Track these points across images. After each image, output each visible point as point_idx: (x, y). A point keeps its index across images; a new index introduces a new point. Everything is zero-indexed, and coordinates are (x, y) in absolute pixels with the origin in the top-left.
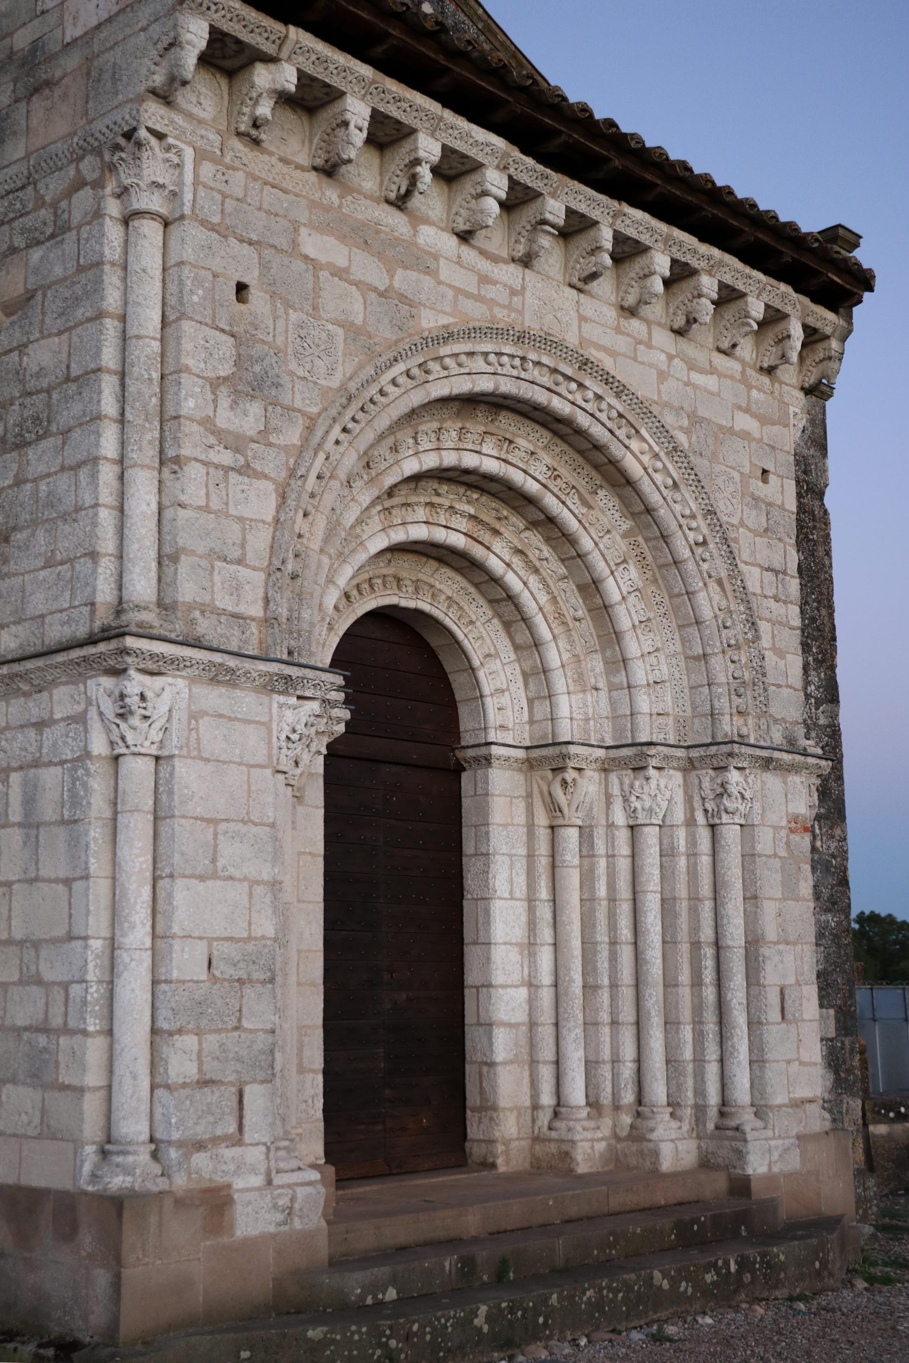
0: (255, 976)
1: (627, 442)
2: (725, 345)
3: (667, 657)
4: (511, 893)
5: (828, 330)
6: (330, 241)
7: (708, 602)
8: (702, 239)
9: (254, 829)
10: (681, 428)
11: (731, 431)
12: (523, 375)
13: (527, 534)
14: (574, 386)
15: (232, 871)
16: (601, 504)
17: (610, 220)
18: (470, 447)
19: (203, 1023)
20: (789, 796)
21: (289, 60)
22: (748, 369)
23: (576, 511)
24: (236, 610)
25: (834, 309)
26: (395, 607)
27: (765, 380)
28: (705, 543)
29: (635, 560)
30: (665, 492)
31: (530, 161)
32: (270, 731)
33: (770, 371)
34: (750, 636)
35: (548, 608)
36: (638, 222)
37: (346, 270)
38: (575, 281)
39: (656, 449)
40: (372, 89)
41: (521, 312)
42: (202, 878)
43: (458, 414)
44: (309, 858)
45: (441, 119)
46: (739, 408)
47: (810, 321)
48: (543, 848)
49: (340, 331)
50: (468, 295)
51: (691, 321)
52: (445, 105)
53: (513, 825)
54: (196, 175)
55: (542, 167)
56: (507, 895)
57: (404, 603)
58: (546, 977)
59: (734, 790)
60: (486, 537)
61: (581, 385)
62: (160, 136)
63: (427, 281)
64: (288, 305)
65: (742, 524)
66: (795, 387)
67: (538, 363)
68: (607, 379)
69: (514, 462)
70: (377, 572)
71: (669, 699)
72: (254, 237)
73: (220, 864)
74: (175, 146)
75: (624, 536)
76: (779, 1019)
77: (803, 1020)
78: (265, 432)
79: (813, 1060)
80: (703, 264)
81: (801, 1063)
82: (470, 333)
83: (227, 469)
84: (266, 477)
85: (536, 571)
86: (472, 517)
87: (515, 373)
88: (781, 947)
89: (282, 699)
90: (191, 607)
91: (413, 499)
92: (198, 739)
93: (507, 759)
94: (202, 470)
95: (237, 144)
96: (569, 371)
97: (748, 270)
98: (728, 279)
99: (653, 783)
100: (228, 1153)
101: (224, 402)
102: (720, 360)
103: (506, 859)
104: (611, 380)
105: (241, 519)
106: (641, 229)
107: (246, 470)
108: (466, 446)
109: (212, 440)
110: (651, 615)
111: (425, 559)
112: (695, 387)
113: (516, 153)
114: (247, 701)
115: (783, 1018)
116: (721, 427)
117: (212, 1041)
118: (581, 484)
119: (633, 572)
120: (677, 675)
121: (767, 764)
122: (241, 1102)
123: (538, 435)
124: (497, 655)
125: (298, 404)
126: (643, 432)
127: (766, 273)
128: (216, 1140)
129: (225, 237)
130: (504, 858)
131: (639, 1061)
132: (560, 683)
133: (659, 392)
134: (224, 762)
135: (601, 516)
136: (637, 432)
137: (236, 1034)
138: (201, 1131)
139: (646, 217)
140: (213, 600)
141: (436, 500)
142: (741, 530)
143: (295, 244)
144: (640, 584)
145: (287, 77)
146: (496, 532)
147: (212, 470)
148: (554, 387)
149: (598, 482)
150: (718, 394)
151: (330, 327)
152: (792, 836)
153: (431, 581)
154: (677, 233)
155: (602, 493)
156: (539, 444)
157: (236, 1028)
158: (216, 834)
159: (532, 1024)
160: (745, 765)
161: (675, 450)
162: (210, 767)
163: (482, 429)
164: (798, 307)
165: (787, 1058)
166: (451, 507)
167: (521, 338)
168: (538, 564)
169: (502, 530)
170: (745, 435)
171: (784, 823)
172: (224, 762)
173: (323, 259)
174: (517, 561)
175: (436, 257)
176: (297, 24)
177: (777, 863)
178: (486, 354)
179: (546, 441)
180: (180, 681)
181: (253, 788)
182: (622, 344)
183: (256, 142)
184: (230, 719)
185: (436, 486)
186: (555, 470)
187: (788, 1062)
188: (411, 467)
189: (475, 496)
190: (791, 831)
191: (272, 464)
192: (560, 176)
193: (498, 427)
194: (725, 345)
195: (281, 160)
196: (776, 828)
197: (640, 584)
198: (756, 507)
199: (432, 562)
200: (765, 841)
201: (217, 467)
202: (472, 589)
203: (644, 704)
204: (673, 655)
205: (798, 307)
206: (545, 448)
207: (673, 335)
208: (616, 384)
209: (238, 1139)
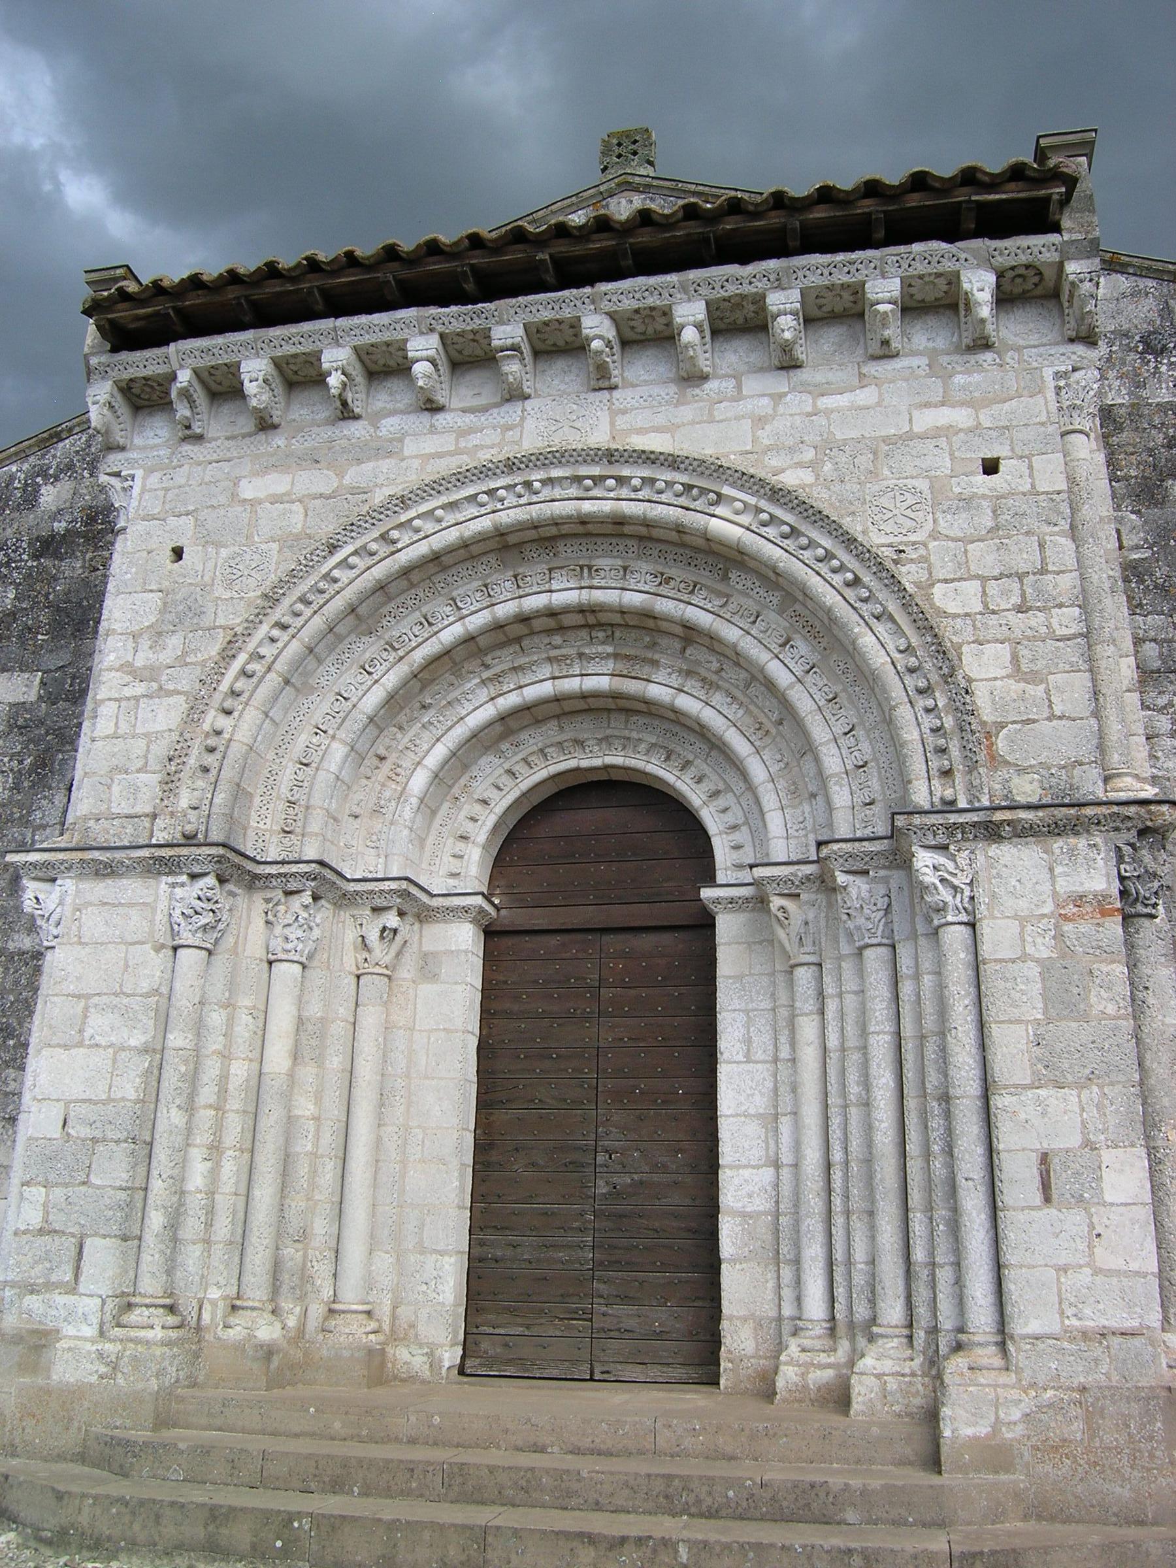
0: (110, 1135)
1: (711, 510)
2: (875, 348)
3: (868, 732)
4: (748, 1055)
5: (1051, 256)
6: (273, 476)
7: (877, 646)
8: (744, 261)
9: (125, 1001)
10: (800, 465)
11: (909, 437)
12: (535, 499)
13: (688, 652)
14: (611, 482)
15: (98, 1039)
16: (739, 587)
17: (592, 307)
18: (535, 589)
19: (52, 1177)
20: (1058, 870)
21: (182, 367)
22: (944, 360)
23: (709, 606)
24: (132, 811)
25: (1056, 228)
26: (577, 769)
27: (989, 356)
28: (856, 582)
29: (804, 632)
30: (786, 543)
31: (454, 309)
32: (154, 910)
33: (983, 344)
34: (946, 670)
35: (748, 720)
36: (631, 292)
37: (288, 494)
38: (593, 383)
39: (752, 500)
40: (260, 345)
41: (518, 443)
42: (66, 1047)
43: (504, 564)
44: (442, 1034)
45: (335, 329)
46: (927, 405)
47: (999, 260)
48: (783, 999)
49: (275, 546)
50: (440, 455)
51: (786, 349)
52: (336, 317)
53: (751, 975)
54: (144, 485)
55: (470, 307)
56: (741, 1057)
57: (585, 764)
58: (786, 1158)
59: (930, 878)
60: (645, 671)
61: (621, 480)
62: (117, 475)
63: (386, 465)
64: (218, 545)
65: (935, 535)
66: (1057, 344)
67: (549, 482)
68: (648, 458)
69: (603, 584)
70: (548, 742)
71: (875, 783)
72: (191, 508)
73: (87, 1035)
74: (129, 475)
75: (781, 613)
76: (1038, 1199)
77: (1104, 1204)
78: (185, 654)
79: (1134, 1266)
80: (760, 285)
81: (1097, 1271)
82: (436, 487)
83: (136, 699)
84: (179, 693)
85: (718, 687)
86: (616, 656)
87: (523, 501)
88: (1042, 1092)
89: (170, 879)
90: (86, 818)
91: (523, 660)
92: (79, 928)
93: (732, 901)
94: (114, 705)
95: (187, 448)
96: (596, 471)
97: (840, 257)
98: (814, 280)
99: (853, 892)
100: (60, 1299)
101: (145, 643)
102: (873, 368)
103: (741, 1018)
104: (652, 456)
105: (146, 735)
106: (637, 296)
107: (163, 692)
108: (528, 590)
109: (128, 678)
110: (838, 688)
111: (605, 715)
112: (828, 412)
113: (433, 311)
114: (131, 888)
115: (1047, 1199)
116: (886, 440)
117: (58, 1193)
118: (704, 577)
119: (802, 647)
120: (883, 749)
121: (991, 832)
122: (80, 1253)
123: (621, 548)
124: (728, 789)
125: (221, 621)
126: (726, 490)
127: (877, 246)
128: (49, 1286)
129: (164, 520)
130: (736, 1014)
131: (872, 1262)
132: (769, 800)
133: (755, 441)
134: (102, 944)
135: (743, 600)
136: (719, 495)
137: (83, 1189)
138: (37, 1274)
139: (641, 280)
140: (109, 808)
141: (554, 653)
142: (932, 545)
143: (234, 495)
144: (815, 658)
145: (184, 377)
146: (655, 663)
147: (124, 704)
148: (585, 495)
149: (720, 566)
150: (879, 404)
151: (264, 546)
152: (1068, 927)
153: (626, 733)
154: (693, 274)
155: (733, 575)
156: (630, 555)
157: (84, 1183)
158: (86, 1008)
159: (777, 1215)
160: (941, 839)
161: (777, 494)
162: (87, 949)
163: (543, 568)
164: (963, 256)
165: (1062, 1262)
166: (581, 655)
167: (510, 466)
168: (714, 678)
169: (656, 657)
170: (947, 431)
171: (1048, 908)
172: (102, 944)
173: (262, 495)
174: (691, 684)
175: (401, 440)
176: (175, 340)
177: (1033, 970)
178: (472, 498)
179: (635, 549)
180: (68, 880)
181: (130, 963)
182: (686, 413)
183: (200, 438)
184: (114, 905)
185: (546, 641)
186: (662, 574)
187: (1063, 1269)
188: (451, 634)
189: (601, 635)
190: (1065, 918)
191: (186, 680)
192: (497, 302)
193: (567, 558)
194: (875, 348)
195: (227, 438)
196: (1022, 921)
197: (815, 658)
198: (967, 509)
199: (613, 716)
200: (998, 937)
201: (128, 699)
202: (677, 729)
203: (841, 796)
204: (874, 728)
205: (963, 256)
206: (639, 557)
207: (783, 373)
208: (662, 457)
209: (72, 1288)
